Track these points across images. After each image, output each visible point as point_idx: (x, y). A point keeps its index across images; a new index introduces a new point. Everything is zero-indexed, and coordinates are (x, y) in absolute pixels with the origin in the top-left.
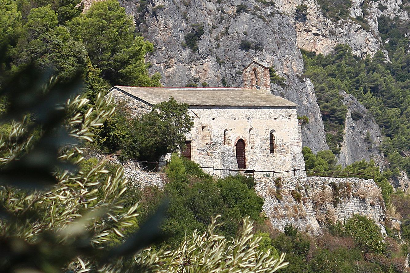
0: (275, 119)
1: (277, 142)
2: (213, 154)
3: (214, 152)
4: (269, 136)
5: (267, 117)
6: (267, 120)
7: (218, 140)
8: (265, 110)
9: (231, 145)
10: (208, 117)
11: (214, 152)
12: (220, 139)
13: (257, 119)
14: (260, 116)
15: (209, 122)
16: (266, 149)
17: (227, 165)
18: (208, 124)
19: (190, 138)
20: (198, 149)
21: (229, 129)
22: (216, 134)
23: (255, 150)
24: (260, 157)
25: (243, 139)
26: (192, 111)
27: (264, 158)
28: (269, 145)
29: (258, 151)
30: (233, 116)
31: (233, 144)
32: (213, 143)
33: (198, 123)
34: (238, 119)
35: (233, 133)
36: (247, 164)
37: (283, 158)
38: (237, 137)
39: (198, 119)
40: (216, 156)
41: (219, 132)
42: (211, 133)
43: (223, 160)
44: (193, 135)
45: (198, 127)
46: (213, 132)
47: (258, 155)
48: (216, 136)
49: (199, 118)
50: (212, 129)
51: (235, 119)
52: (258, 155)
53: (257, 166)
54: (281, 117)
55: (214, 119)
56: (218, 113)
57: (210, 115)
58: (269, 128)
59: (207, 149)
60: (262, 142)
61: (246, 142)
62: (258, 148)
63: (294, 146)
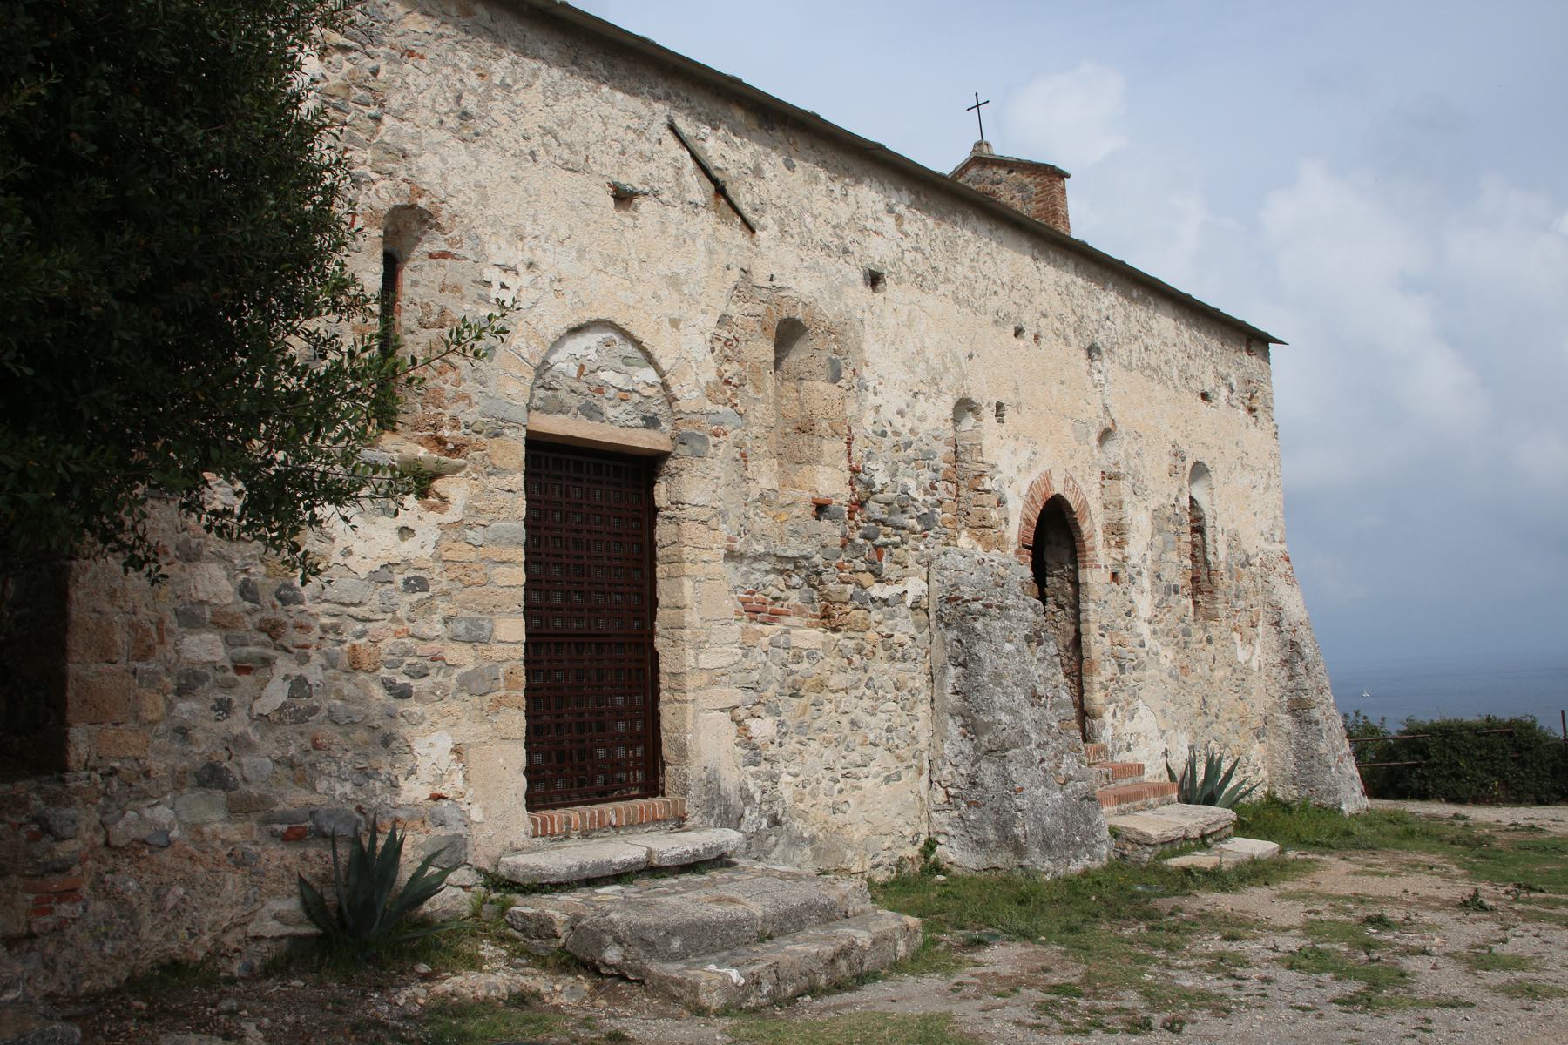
1: (1220, 553)
2: (876, 615)
3: (877, 590)
4: (1185, 502)
5: (1175, 373)
7: (912, 484)
8: (1165, 324)
9: (1000, 543)
10: (826, 247)
11: (877, 590)
12: (927, 476)
14: (1144, 355)
15: (837, 292)
17: (1005, 718)
18: (829, 309)
19: (651, 422)
20: (731, 555)
21: (983, 394)
22: (898, 421)
25: (1069, 497)
26: (672, 128)
30: (1003, 302)
32: (874, 509)
33: (735, 275)
34: (1037, 337)
35: (1012, 443)
38: (1035, 475)
39: (739, 237)
41: (921, 406)
42: (852, 409)
43: (952, 671)
44: (690, 396)
45: (734, 310)
46: (870, 396)
47: (1145, 630)
49: (750, 228)
50: (866, 373)
53: (1143, 711)
54: (1224, 392)
56: (906, 244)
57: (849, 235)
59: (818, 559)
60: (1158, 539)
61: (1085, 527)
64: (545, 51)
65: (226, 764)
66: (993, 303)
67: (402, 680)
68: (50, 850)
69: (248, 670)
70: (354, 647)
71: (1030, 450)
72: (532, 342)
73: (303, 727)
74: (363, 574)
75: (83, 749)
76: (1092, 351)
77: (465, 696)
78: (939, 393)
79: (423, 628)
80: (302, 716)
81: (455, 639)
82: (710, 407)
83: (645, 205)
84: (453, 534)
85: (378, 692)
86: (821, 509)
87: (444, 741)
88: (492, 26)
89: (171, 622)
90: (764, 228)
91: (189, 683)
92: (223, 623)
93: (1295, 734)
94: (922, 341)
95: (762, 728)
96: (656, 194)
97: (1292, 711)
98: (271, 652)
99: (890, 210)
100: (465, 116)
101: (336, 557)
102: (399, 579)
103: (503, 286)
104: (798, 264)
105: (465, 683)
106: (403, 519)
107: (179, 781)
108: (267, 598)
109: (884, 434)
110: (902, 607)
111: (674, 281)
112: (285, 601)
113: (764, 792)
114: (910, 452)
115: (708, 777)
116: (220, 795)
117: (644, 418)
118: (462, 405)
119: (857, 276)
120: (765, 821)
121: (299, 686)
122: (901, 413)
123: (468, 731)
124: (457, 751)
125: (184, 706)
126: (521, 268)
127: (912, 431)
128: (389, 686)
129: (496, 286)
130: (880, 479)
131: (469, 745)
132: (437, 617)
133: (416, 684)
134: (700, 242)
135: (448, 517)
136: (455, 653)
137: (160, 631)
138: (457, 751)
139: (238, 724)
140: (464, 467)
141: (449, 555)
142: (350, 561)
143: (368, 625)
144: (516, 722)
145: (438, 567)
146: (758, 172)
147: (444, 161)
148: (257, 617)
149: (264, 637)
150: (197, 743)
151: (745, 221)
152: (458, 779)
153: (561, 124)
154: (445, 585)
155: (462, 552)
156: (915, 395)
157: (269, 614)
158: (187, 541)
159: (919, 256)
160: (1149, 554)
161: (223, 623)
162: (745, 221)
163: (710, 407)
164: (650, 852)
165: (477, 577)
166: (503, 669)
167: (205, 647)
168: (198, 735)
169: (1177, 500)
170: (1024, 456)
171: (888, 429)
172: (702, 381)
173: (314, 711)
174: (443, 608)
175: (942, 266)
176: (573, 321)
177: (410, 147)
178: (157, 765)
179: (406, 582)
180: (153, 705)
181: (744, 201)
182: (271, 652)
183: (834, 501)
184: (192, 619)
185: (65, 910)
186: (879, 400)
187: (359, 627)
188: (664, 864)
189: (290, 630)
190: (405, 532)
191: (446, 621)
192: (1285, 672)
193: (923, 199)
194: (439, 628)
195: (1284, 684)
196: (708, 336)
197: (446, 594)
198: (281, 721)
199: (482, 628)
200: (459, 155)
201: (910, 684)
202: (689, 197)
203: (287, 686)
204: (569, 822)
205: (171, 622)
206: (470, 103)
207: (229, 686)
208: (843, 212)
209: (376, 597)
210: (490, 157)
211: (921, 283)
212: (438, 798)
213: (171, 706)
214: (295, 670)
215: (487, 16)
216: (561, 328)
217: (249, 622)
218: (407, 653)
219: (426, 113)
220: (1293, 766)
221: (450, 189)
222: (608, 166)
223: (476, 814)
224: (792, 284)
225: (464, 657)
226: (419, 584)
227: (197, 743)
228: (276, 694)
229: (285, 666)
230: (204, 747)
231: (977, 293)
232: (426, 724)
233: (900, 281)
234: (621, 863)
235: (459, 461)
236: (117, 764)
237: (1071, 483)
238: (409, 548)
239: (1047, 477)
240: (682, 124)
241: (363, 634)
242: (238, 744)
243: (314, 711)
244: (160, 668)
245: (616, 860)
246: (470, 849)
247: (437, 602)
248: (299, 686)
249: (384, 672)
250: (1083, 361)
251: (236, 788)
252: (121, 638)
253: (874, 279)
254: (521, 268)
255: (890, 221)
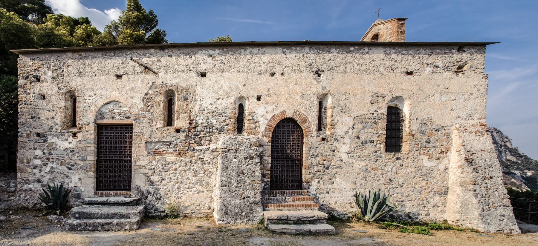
0: (409, 73)
3: (197, 148)
6: (379, 75)
11: (197, 148)
12: (221, 119)
13: (346, 72)
16: (372, 142)
18: (183, 85)
22: (210, 107)
23: (336, 144)
24: (351, 160)
25: (295, 117)
26: (132, 59)
27: (363, 164)
28: (385, 132)
29: (344, 148)
30: (263, 68)
31: (262, 129)
32: (199, 129)
36: (305, 177)
37: (427, 163)
38: (276, 113)
39: (152, 76)
40: (205, 158)
41: (219, 102)
42: (190, 106)
46: (199, 102)
48: (206, 111)
51: (273, 74)
52: (345, 157)
55: (203, 75)
56: (216, 63)
57: (191, 67)
58: (386, 93)
62: (347, 140)
63: (471, 132)
64: (98, 56)
65: (41, 179)
66: (260, 68)
67: (70, 167)
68: (9, 189)
69: (45, 165)
70: (62, 162)
71: (274, 106)
72: (95, 108)
73: (53, 174)
74: (62, 150)
75: (19, 176)
76: (318, 73)
77: (81, 169)
78: (228, 97)
79: (73, 158)
80: (53, 173)
81: (79, 160)
82: (141, 112)
83: (124, 77)
84: (79, 143)
85: (66, 169)
86: (178, 131)
87: (77, 177)
88: (86, 55)
89: (32, 158)
90: (161, 72)
91: (35, 167)
92: (40, 158)
93: (462, 194)
94: (222, 85)
95: (155, 178)
96: (127, 74)
97: (461, 185)
98: (48, 162)
99: (210, 56)
100: (81, 72)
101: (58, 148)
102: (69, 150)
103: (89, 99)
104: (172, 77)
105: (81, 167)
106: (69, 141)
107: (34, 181)
108: (47, 154)
109: (204, 110)
110: (208, 151)
111: (132, 89)
112: (50, 155)
113: (155, 192)
114: (214, 114)
115: (137, 187)
116: (40, 184)
117: (126, 117)
118: (80, 121)
119: (195, 75)
120: (154, 198)
121: (52, 168)
122: (212, 105)
123: (82, 176)
124: (80, 179)
125: (35, 171)
126: (93, 95)
127: (215, 108)
128: (68, 168)
129: (88, 99)
130: (200, 122)
131: (82, 178)
132: (76, 156)
133: (72, 168)
134: (139, 80)
135: (78, 140)
136: (79, 162)
137: (31, 160)
138: (80, 179)
139: (43, 173)
140: (82, 131)
141: (78, 146)
142: (60, 148)
143: (64, 158)
144: (92, 174)
145: (76, 148)
146: (159, 61)
147: (76, 81)
148: (46, 157)
149: (47, 160)
150: (37, 176)
151: (154, 72)
152: (80, 184)
153: (102, 68)
154: (77, 151)
155: (80, 145)
156: (218, 99)
157: (47, 157)
158: (35, 147)
159: (222, 65)
160: (351, 131)
161: (40, 158)
162: (154, 72)
163: (141, 112)
164: (107, 200)
165: (84, 149)
166: (89, 165)
167: (37, 162)
168: (37, 175)
169: (376, 111)
170: (270, 108)
171: (206, 109)
172: (139, 108)
173: (55, 171)
174: (77, 155)
175: (233, 65)
176: (105, 102)
177: (69, 81)
178: (30, 179)
179: (70, 151)
180: (29, 170)
181: (154, 68)
182: (48, 162)
183: (183, 128)
184: (35, 158)
185: (12, 198)
186: (202, 103)
187: (62, 158)
188: (111, 202)
189: (51, 159)
190: (70, 143)
191: (78, 157)
192: (460, 170)
193: (225, 50)
194: (76, 158)
195: (459, 175)
196: (141, 98)
197: (77, 152)
198: (49, 173)
199: (84, 158)
200: (79, 79)
201: (210, 170)
202: (136, 72)
203: (50, 168)
204: (102, 193)
205: (32, 158)
206: (81, 70)
207: (41, 167)
208: (190, 61)
209: (65, 154)
210: (86, 78)
211: (223, 71)
212: (76, 187)
213: (33, 170)
214: (51, 165)
215: (84, 54)
216: (102, 104)
217: (45, 158)
218: (70, 162)
219: (72, 75)
220: (459, 207)
221: (77, 86)
222: (115, 72)
223: (83, 190)
224: (170, 82)
225: (81, 163)
226: (73, 151)
227: (37, 176)
228: (48, 169)
229: (50, 165)
230: (37, 177)
231: (249, 68)
232: (74, 174)
233: (213, 72)
234: (100, 201)
235: (81, 130)
236: (24, 178)
237: (298, 113)
238: (71, 145)
239: (283, 113)
240: (135, 58)
241: (63, 160)
242: (43, 176)
243: (55, 171)
244: (31, 165)
245: (99, 200)
246: (82, 196)
247: (76, 154)
248: (52, 168)
249: (67, 165)
250: (312, 76)
251: (43, 183)
252: (25, 161)
253: (203, 75)
254: (93, 95)
255: (209, 60)
